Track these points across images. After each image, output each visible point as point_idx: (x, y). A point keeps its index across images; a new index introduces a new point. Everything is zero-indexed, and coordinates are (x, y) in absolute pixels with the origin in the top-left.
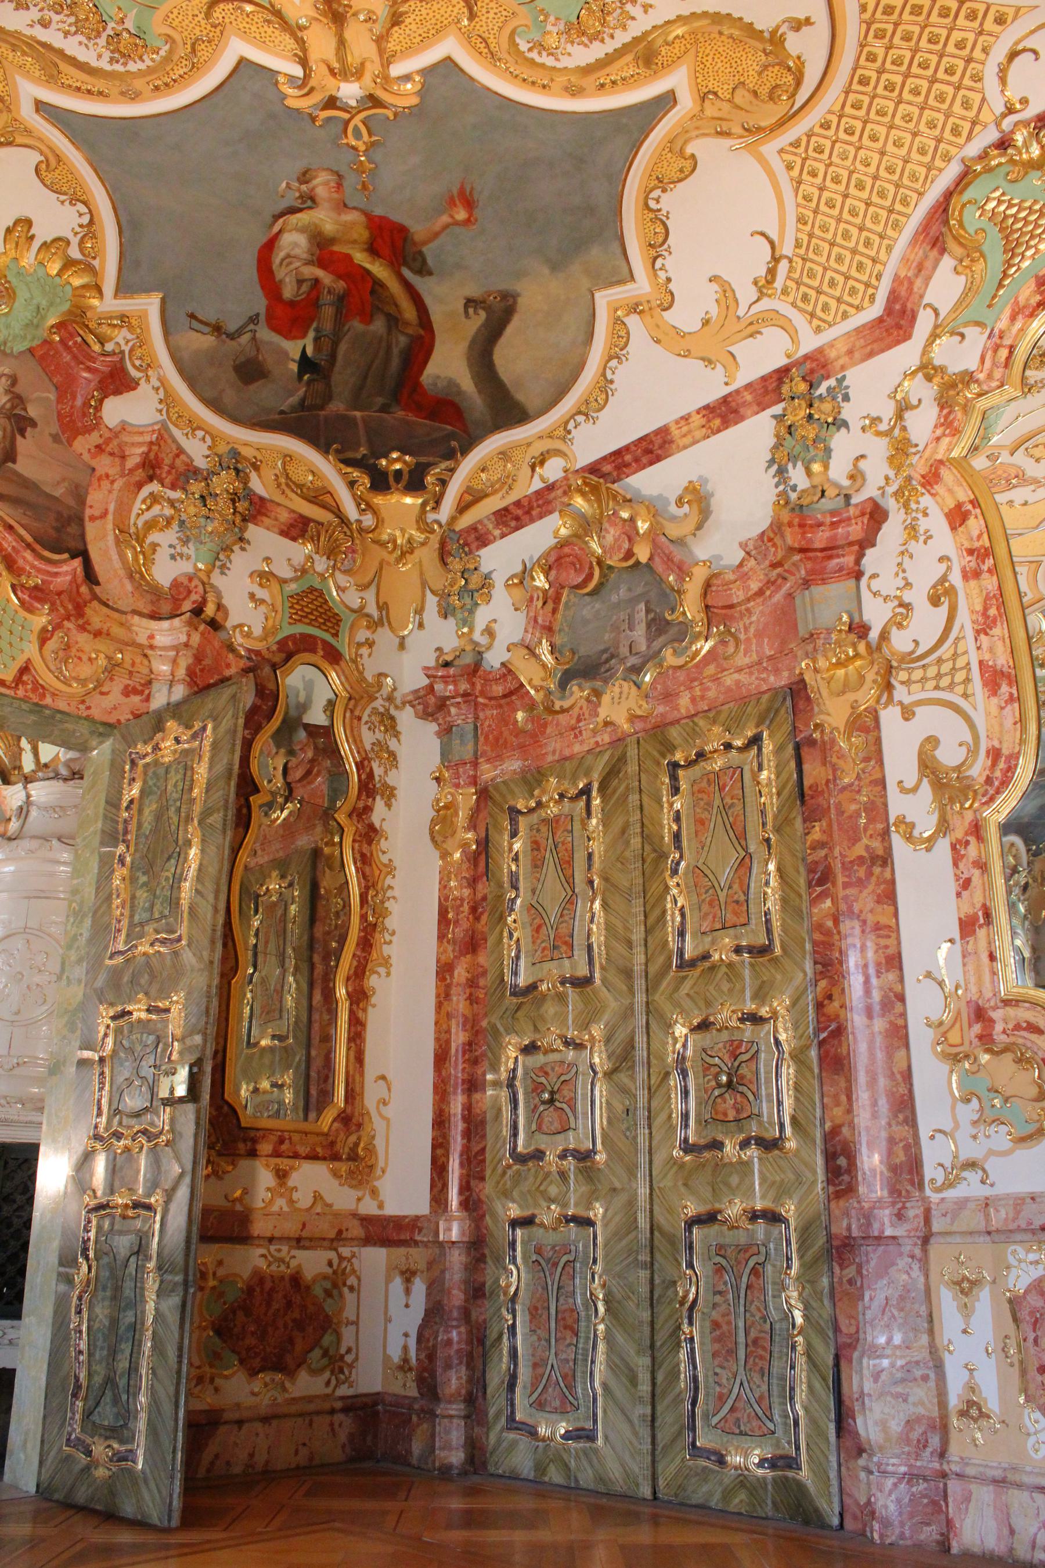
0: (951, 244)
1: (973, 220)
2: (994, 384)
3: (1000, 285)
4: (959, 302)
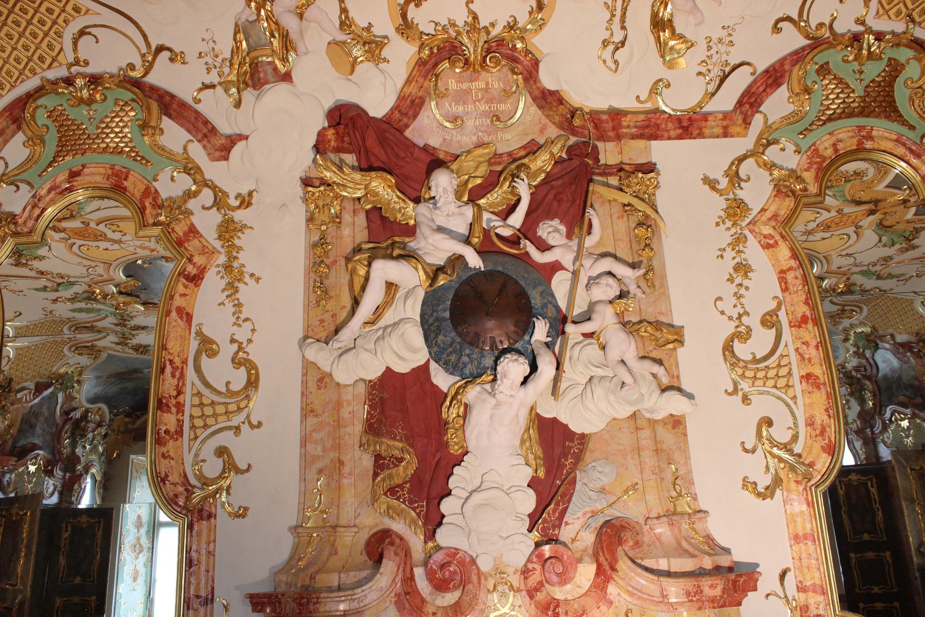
0: (24, 126)
1: (42, 117)
2: (26, 230)
3: (50, 165)
4: (22, 165)
